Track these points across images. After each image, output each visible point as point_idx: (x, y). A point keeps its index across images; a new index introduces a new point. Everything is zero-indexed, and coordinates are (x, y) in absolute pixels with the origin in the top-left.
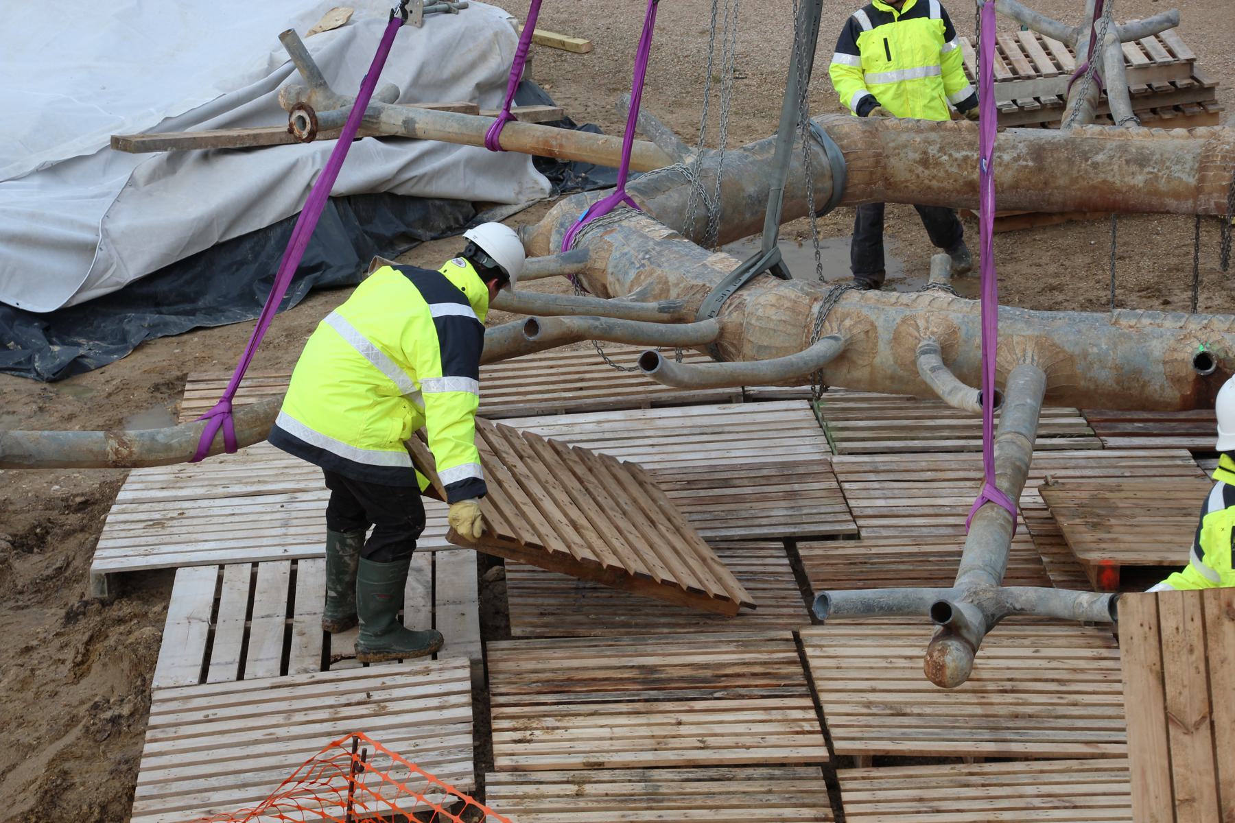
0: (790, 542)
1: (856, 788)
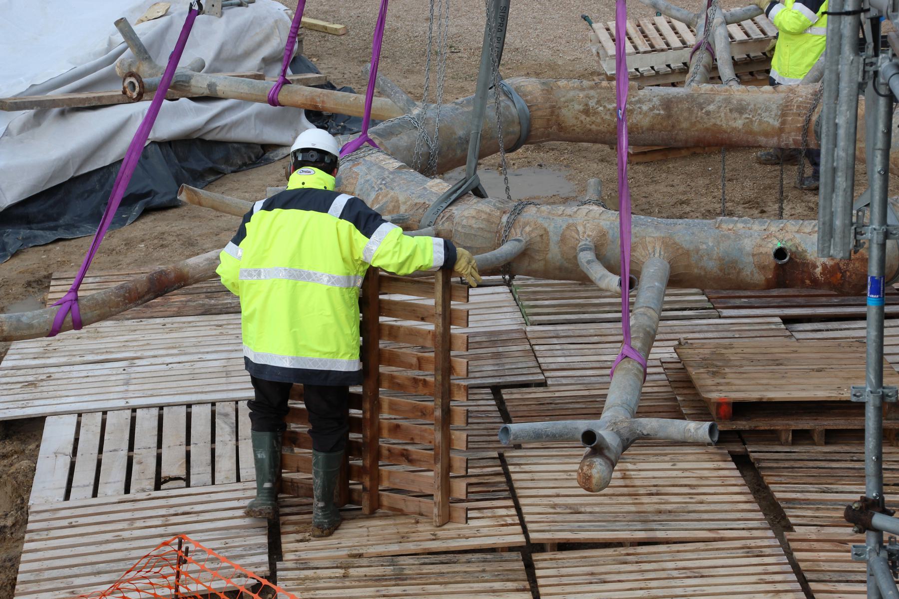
0: (496, 390)
1: (547, 567)
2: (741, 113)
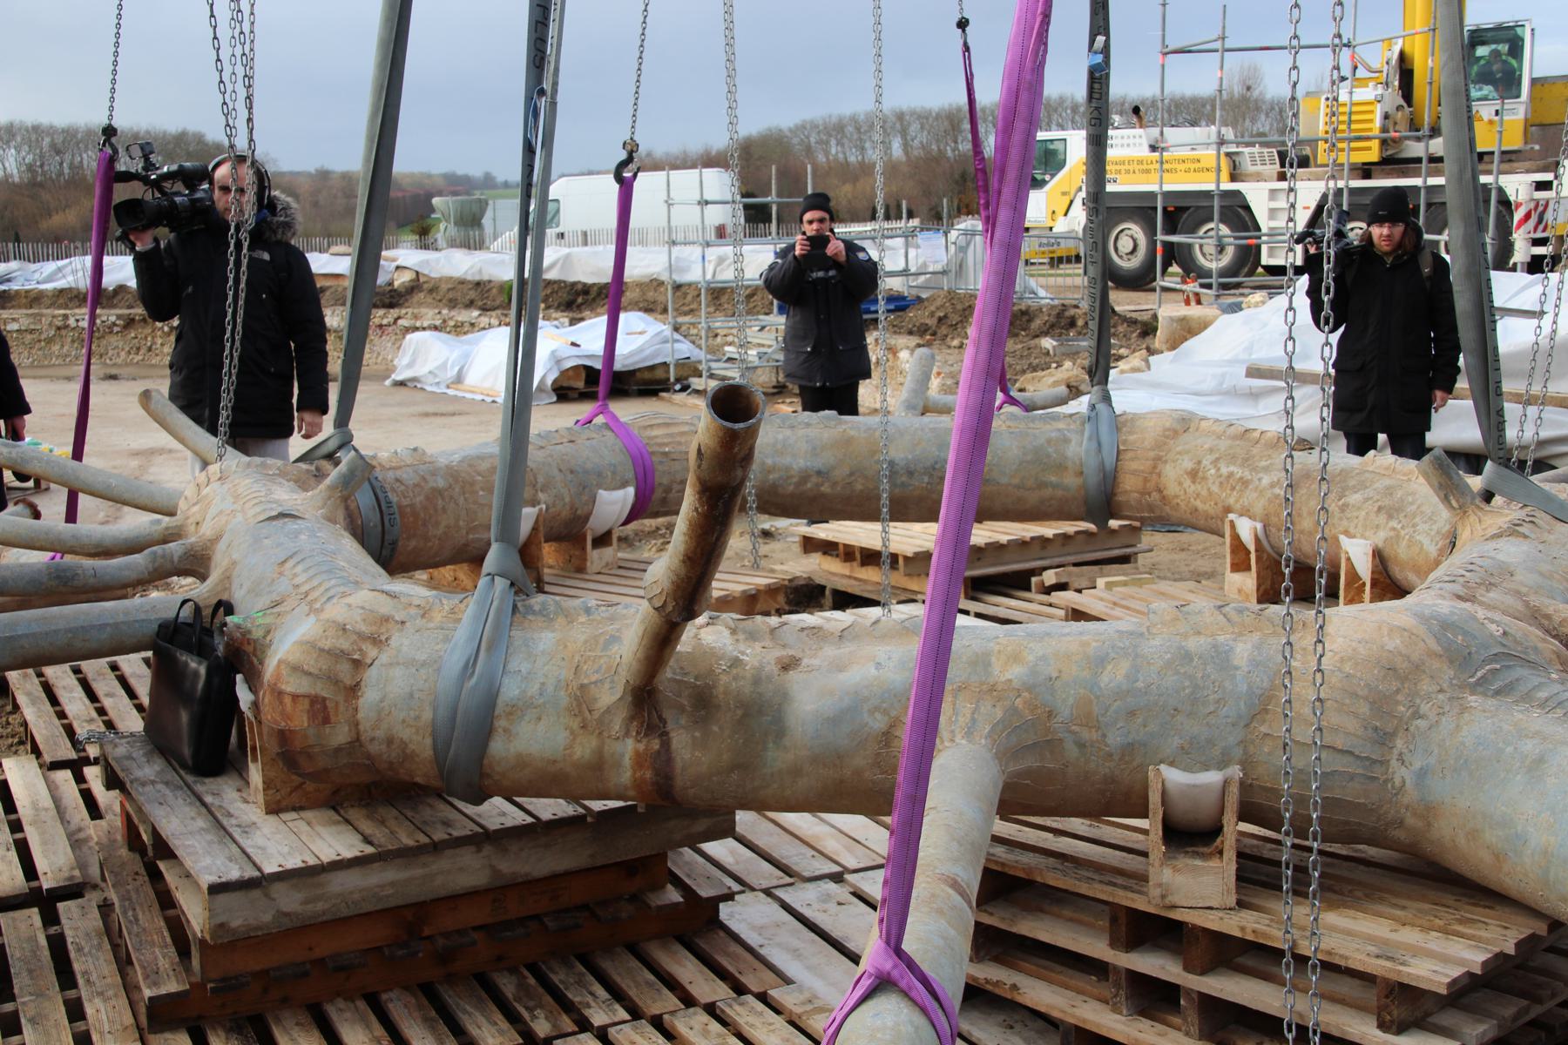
2: (1390, 517)
